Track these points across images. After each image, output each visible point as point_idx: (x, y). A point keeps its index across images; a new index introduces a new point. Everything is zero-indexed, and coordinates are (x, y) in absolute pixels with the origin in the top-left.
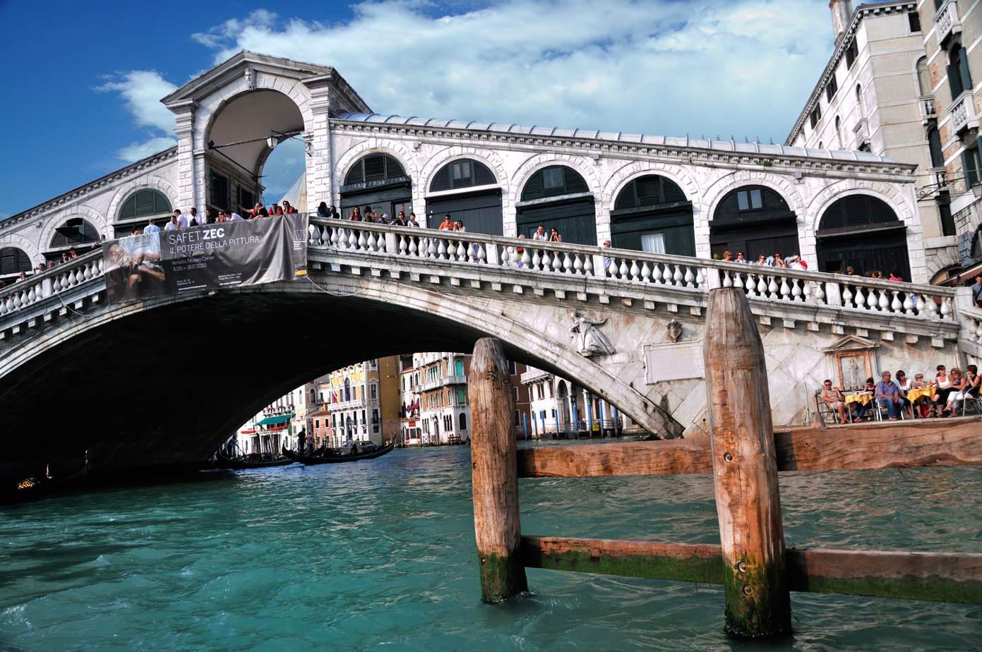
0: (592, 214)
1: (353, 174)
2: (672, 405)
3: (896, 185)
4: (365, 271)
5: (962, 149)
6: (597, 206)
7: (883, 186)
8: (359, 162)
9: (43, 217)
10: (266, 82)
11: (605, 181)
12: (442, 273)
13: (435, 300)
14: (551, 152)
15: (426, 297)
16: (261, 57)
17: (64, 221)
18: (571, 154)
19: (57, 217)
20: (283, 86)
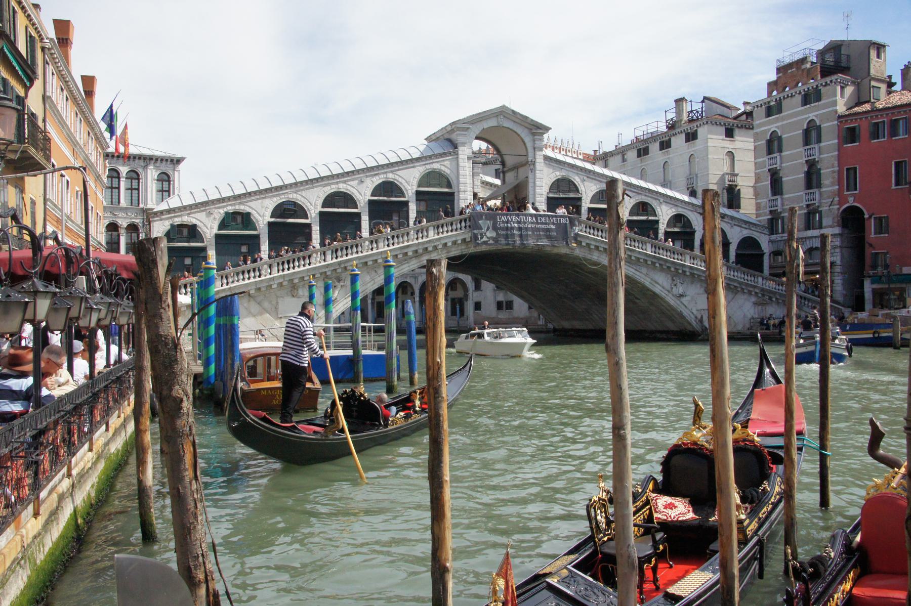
5: (769, 217)
6: (660, 225)
9: (367, 177)
10: (507, 124)
11: (664, 214)
16: (513, 111)
17: (380, 181)
19: (374, 179)
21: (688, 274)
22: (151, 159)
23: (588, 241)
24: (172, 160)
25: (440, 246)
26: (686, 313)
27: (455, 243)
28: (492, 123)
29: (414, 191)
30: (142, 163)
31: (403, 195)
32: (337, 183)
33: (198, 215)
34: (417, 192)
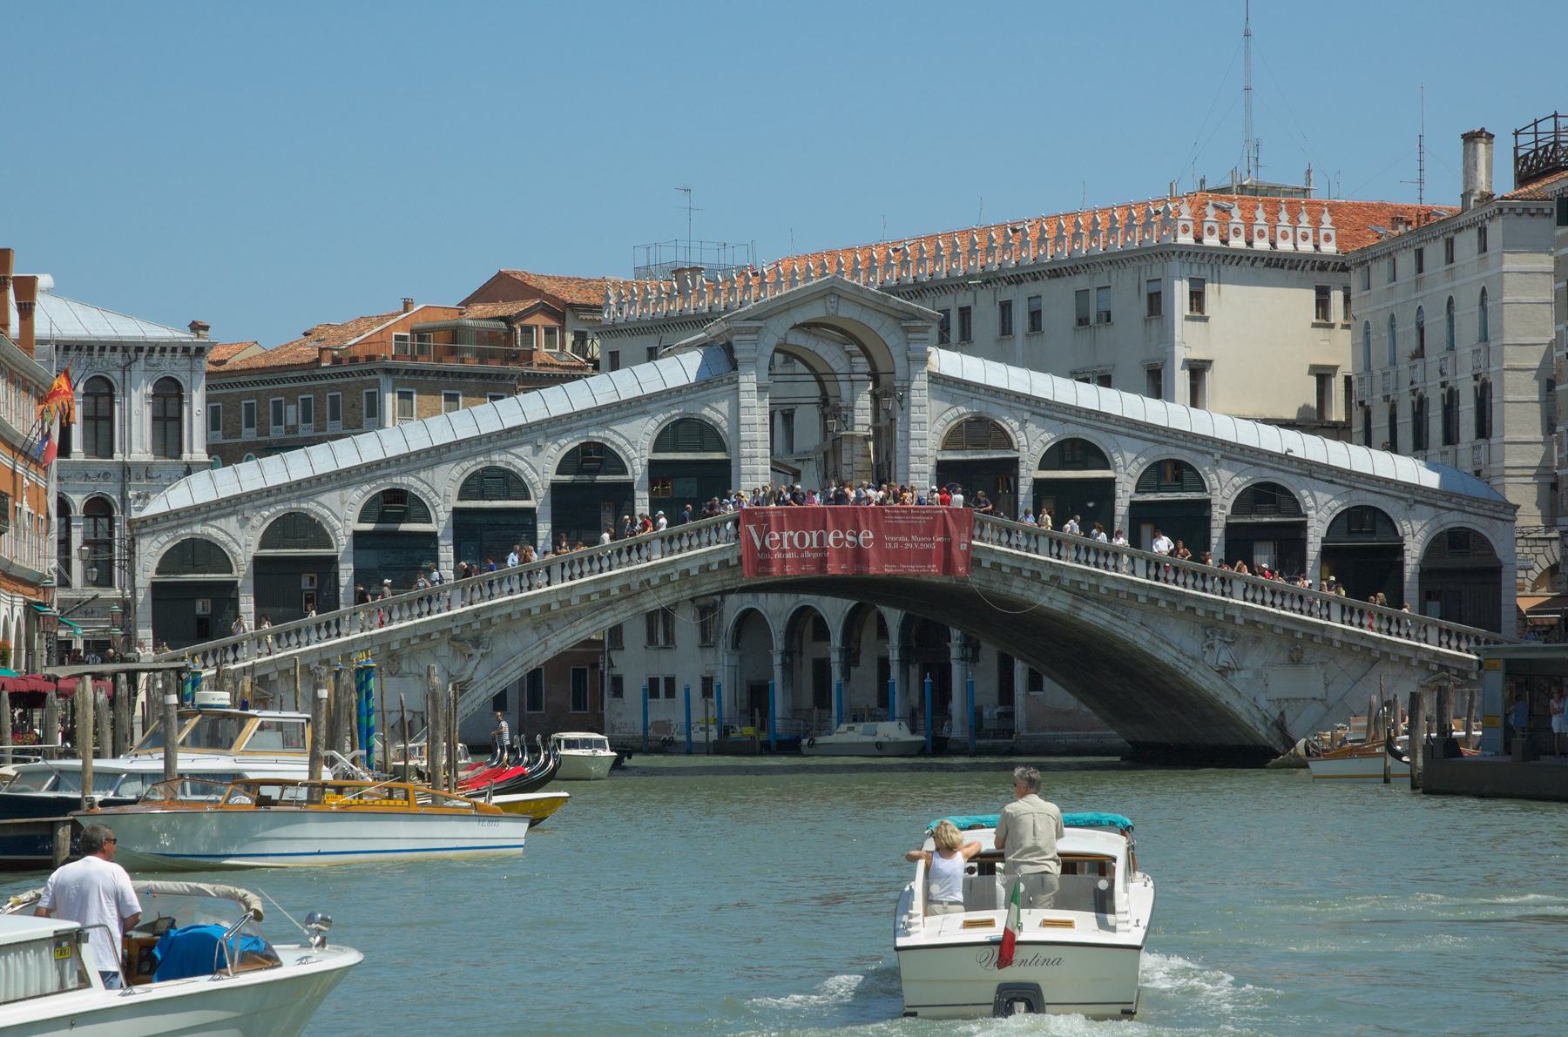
0: (1208, 519)
1: (951, 441)
2: (1288, 720)
3: (1499, 523)
4: (1018, 571)
7: (1486, 522)
8: (959, 425)
9: (547, 437)
10: (847, 312)
12: (1093, 581)
13: (1078, 604)
14: (1171, 444)
15: (1069, 600)
17: (576, 444)
18: (1191, 449)
19: (563, 441)
20: (874, 322)
21: (1239, 621)
22: (139, 349)
23: (993, 559)
24: (186, 349)
25: (676, 577)
26: (1239, 707)
27: (705, 569)
28: (815, 312)
29: (645, 462)
30: (118, 357)
31: (624, 471)
32: (489, 452)
33: (221, 523)
34: (650, 461)
